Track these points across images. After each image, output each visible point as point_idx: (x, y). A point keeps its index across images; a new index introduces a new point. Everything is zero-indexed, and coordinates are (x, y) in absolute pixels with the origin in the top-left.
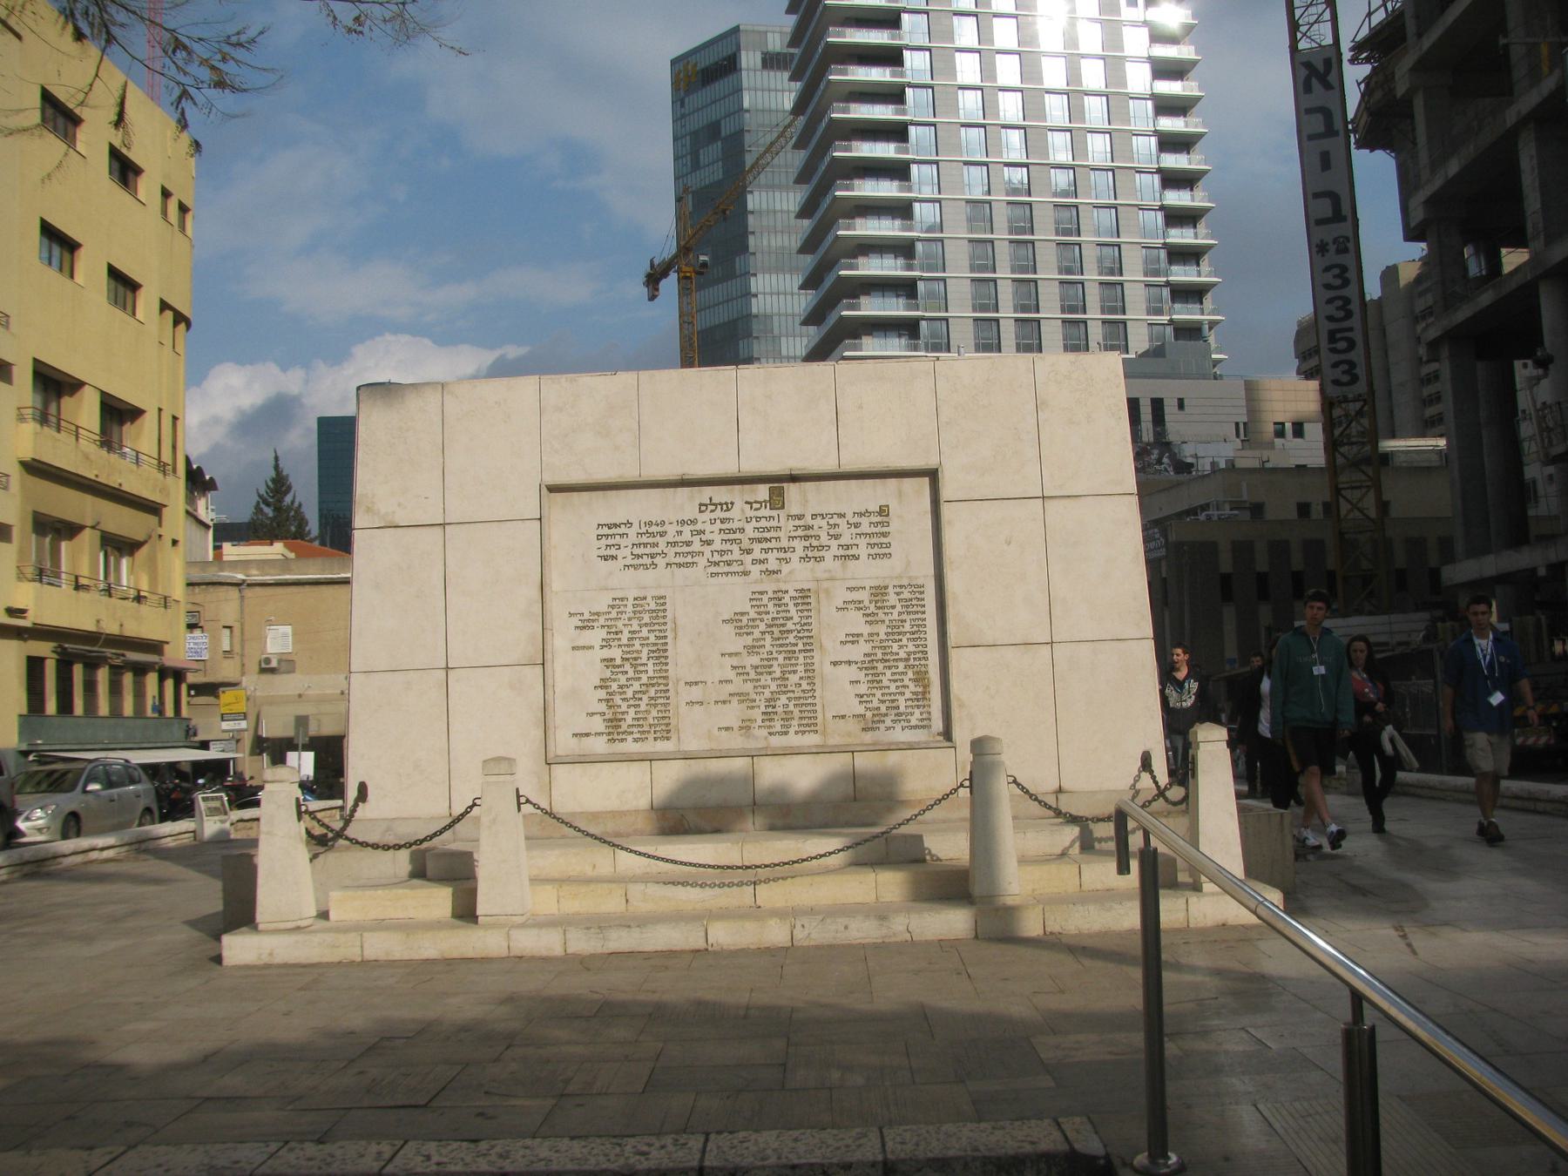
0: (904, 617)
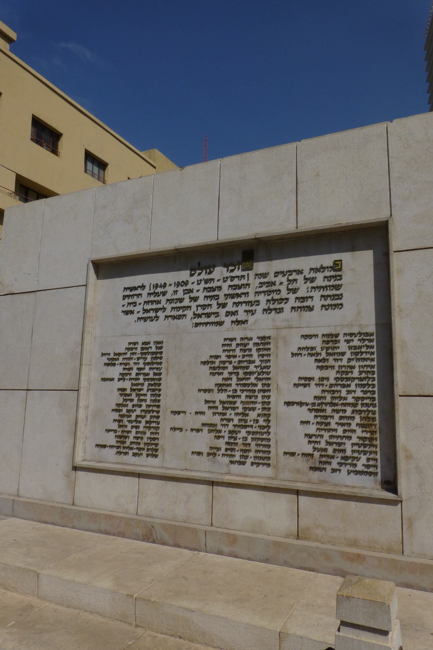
0: (353, 363)
